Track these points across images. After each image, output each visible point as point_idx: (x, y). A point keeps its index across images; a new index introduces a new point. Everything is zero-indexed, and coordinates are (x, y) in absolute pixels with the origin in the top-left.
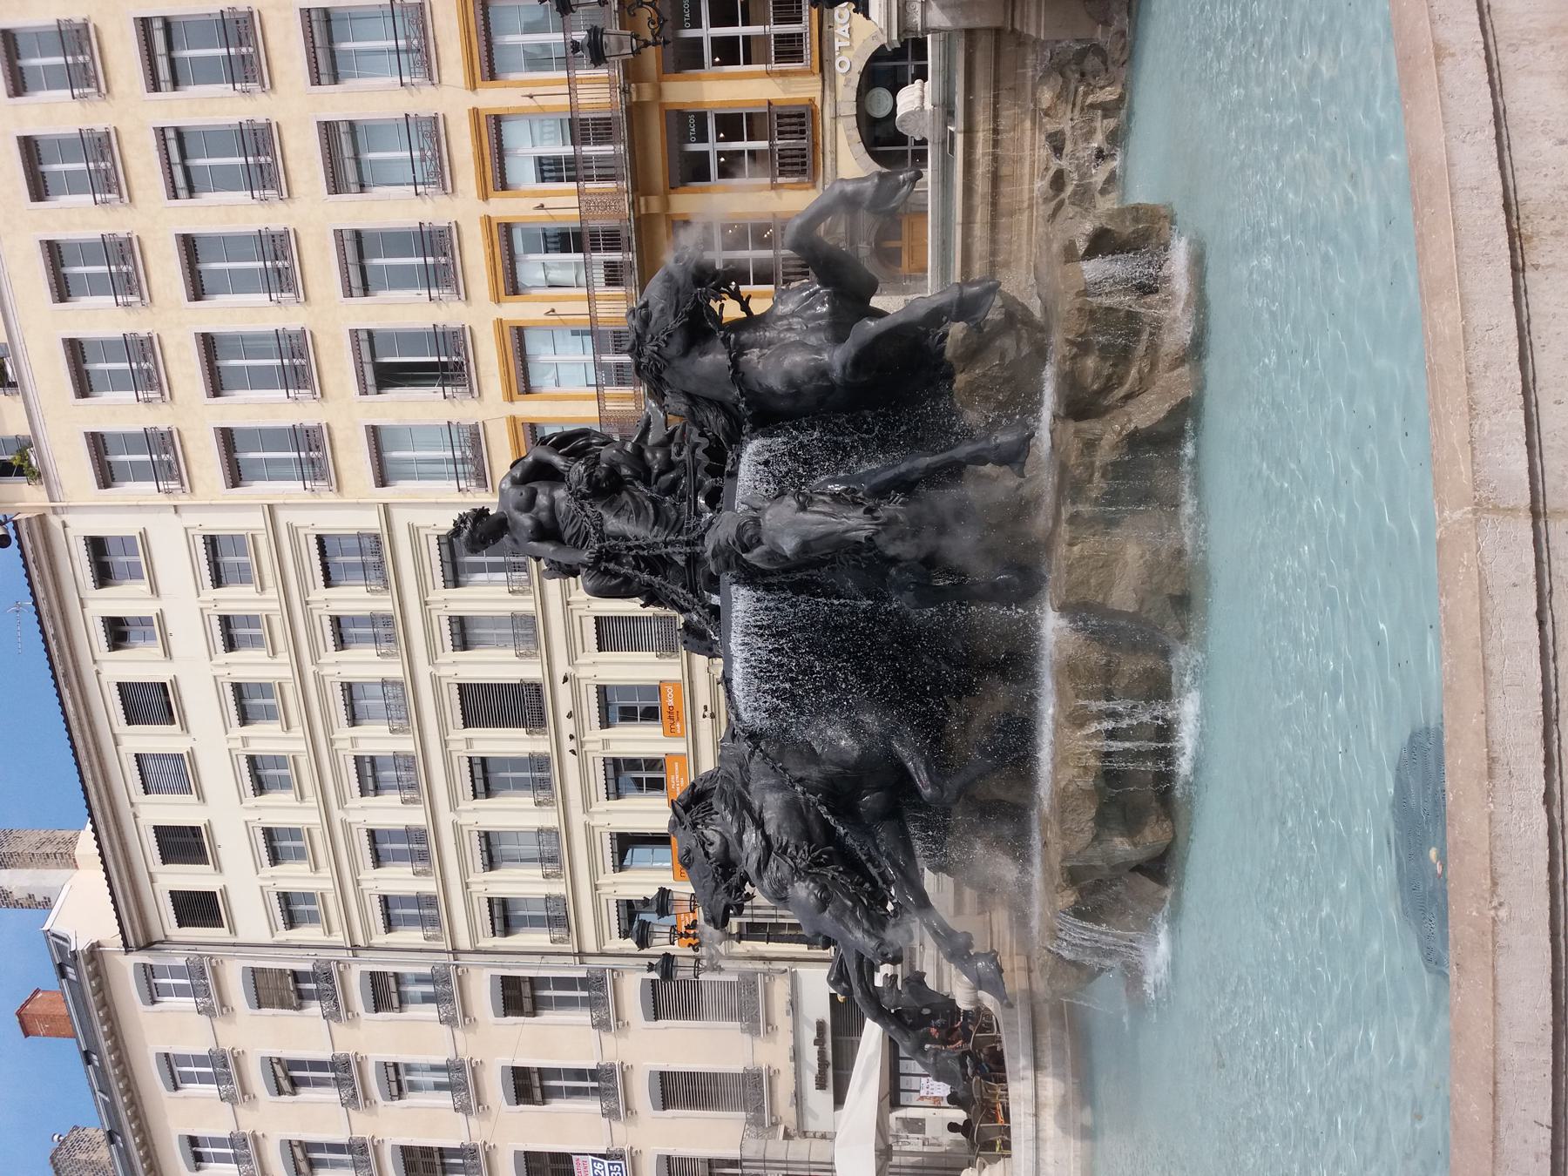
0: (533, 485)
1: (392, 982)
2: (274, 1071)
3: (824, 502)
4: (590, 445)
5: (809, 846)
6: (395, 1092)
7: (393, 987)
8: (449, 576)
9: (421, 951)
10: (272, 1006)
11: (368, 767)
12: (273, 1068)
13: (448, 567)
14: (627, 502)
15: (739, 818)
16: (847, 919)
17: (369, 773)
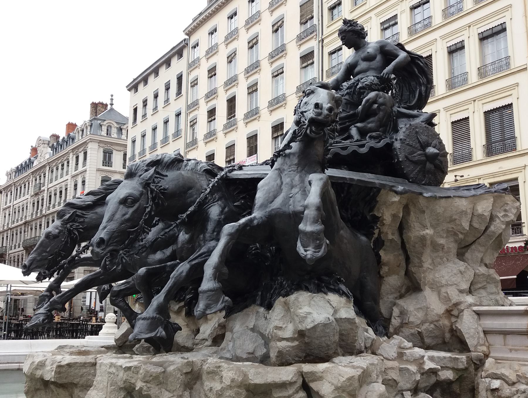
0: (379, 58)
1: (311, 61)
2: (278, 22)
3: (124, 215)
4: (420, 85)
5: (80, 228)
6: (275, 74)
7: (309, 62)
8: (485, 34)
9: (322, 70)
10: (301, 11)
11: (393, 22)
12: (280, 21)
13: (490, 32)
14: (349, 112)
15: (101, 192)
16: (41, 249)
17: (391, 23)
